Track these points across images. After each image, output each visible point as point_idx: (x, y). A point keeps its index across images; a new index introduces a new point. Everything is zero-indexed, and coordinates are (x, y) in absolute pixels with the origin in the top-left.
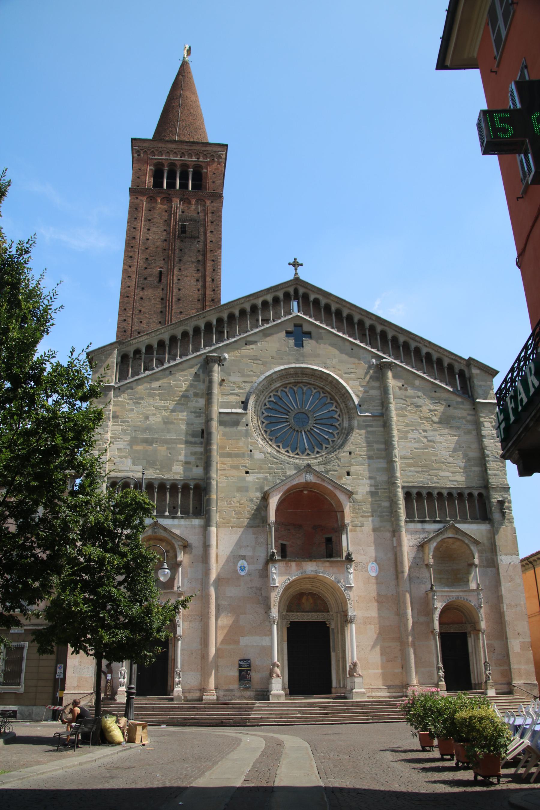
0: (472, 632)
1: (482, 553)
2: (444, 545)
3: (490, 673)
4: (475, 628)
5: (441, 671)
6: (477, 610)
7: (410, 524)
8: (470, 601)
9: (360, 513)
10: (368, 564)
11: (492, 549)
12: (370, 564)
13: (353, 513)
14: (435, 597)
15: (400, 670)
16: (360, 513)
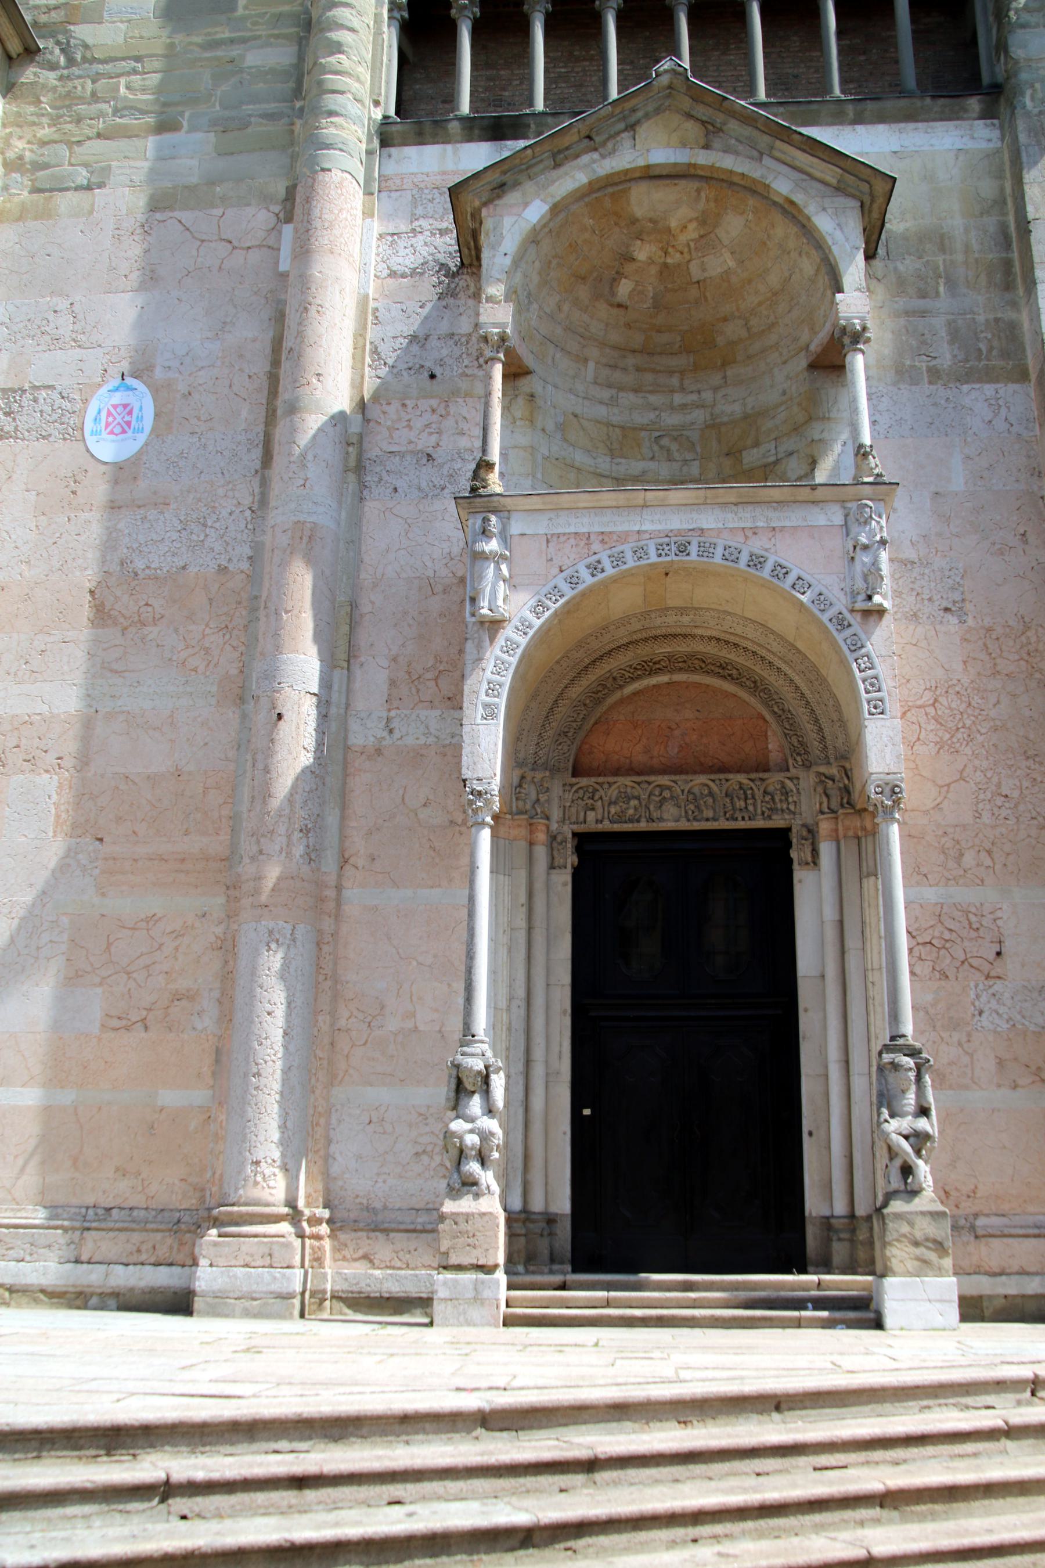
0: (825, 827)
1: (923, 295)
2: (642, 252)
3: (919, 1140)
4: (847, 791)
5: (475, 1105)
6: (839, 637)
7: (411, 151)
8: (781, 571)
9: (101, 114)
10: (87, 392)
11: (1008, 264)
12: (103, 390)
13: (55, 121)
14: (493, 545)
15: (199, 1096)
16: (101, 114)
